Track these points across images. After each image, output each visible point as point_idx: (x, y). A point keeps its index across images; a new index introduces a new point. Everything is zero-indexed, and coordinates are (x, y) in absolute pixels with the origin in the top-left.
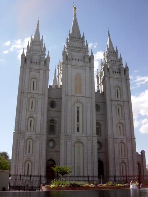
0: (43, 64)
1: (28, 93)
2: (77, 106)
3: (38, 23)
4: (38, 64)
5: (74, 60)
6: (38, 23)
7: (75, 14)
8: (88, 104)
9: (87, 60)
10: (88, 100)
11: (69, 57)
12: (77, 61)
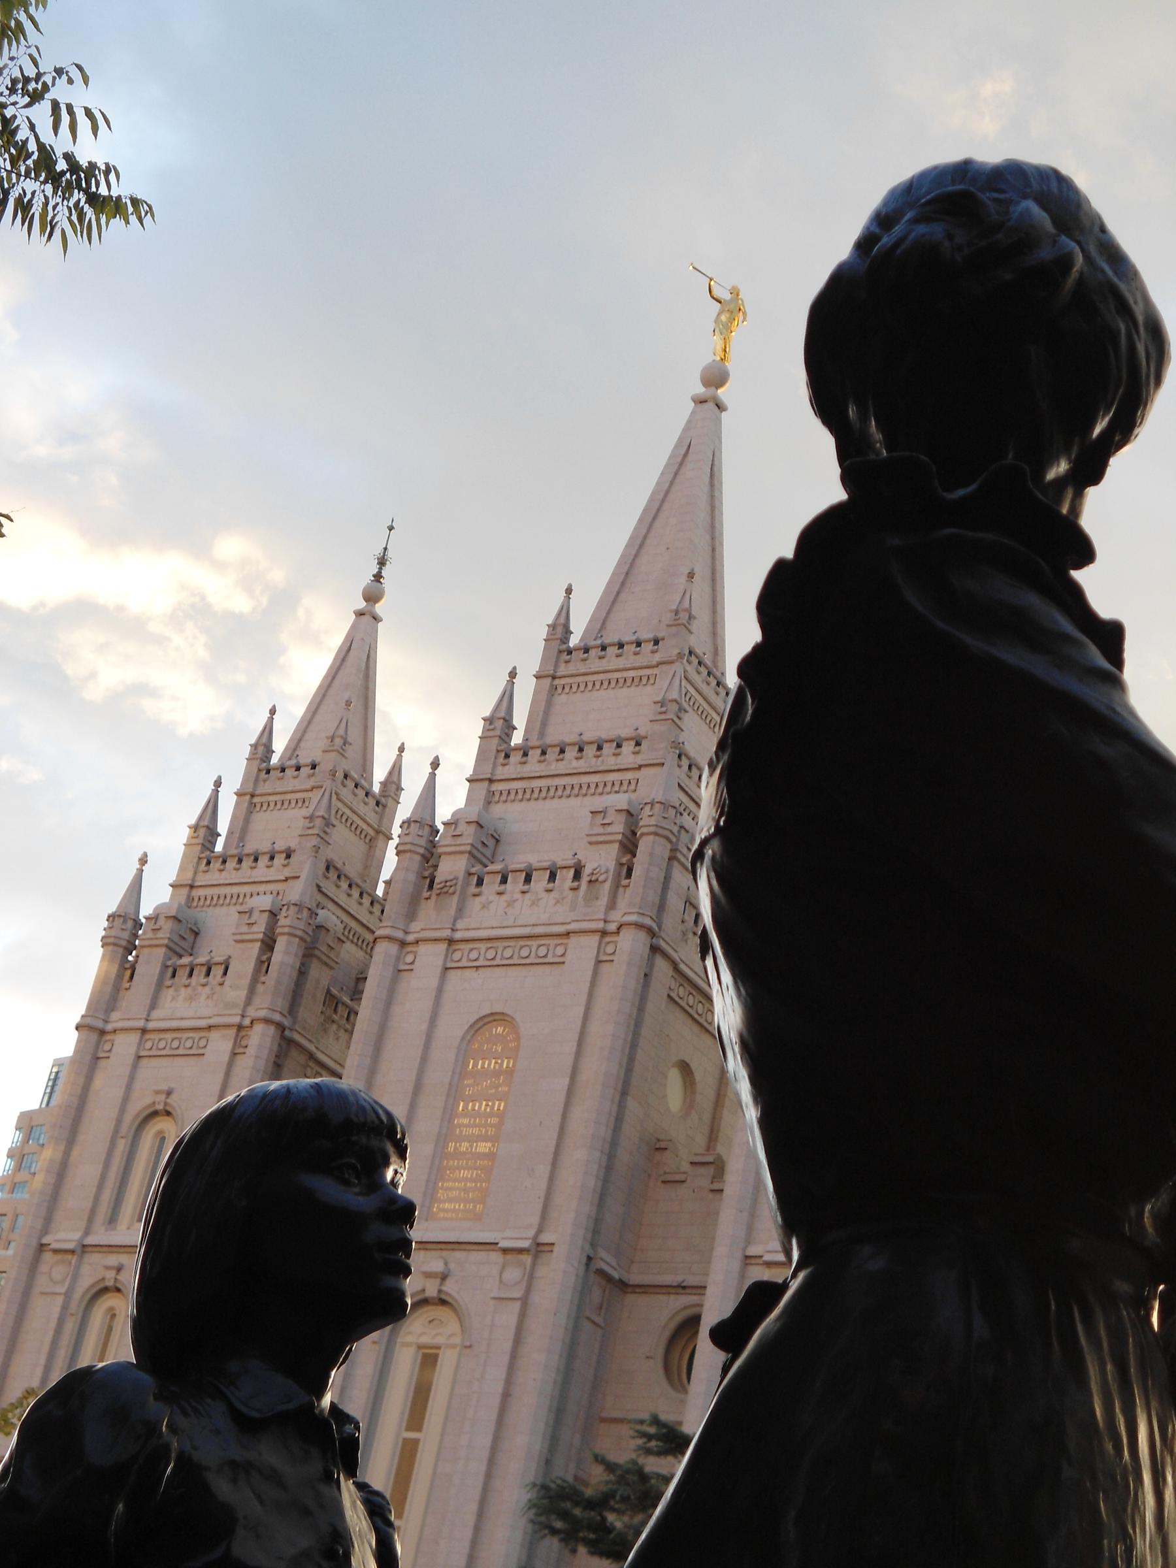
0: (250, 966)
1: (85, 1248)
2: (424, 1340)
3: (378, 577)
4: (217, 971)
5: (491, 885)
6: (378, 577)
7: (716, 377)
8: (509, 1317)
9: (603, 860)
10: (513, 1274)
11: (451, 868)
12: (515, 884)
